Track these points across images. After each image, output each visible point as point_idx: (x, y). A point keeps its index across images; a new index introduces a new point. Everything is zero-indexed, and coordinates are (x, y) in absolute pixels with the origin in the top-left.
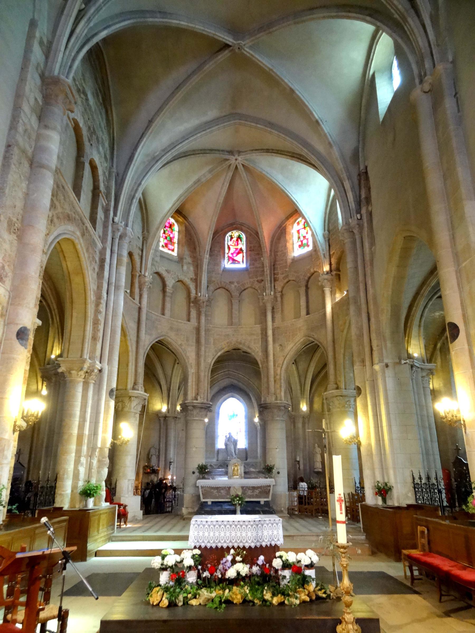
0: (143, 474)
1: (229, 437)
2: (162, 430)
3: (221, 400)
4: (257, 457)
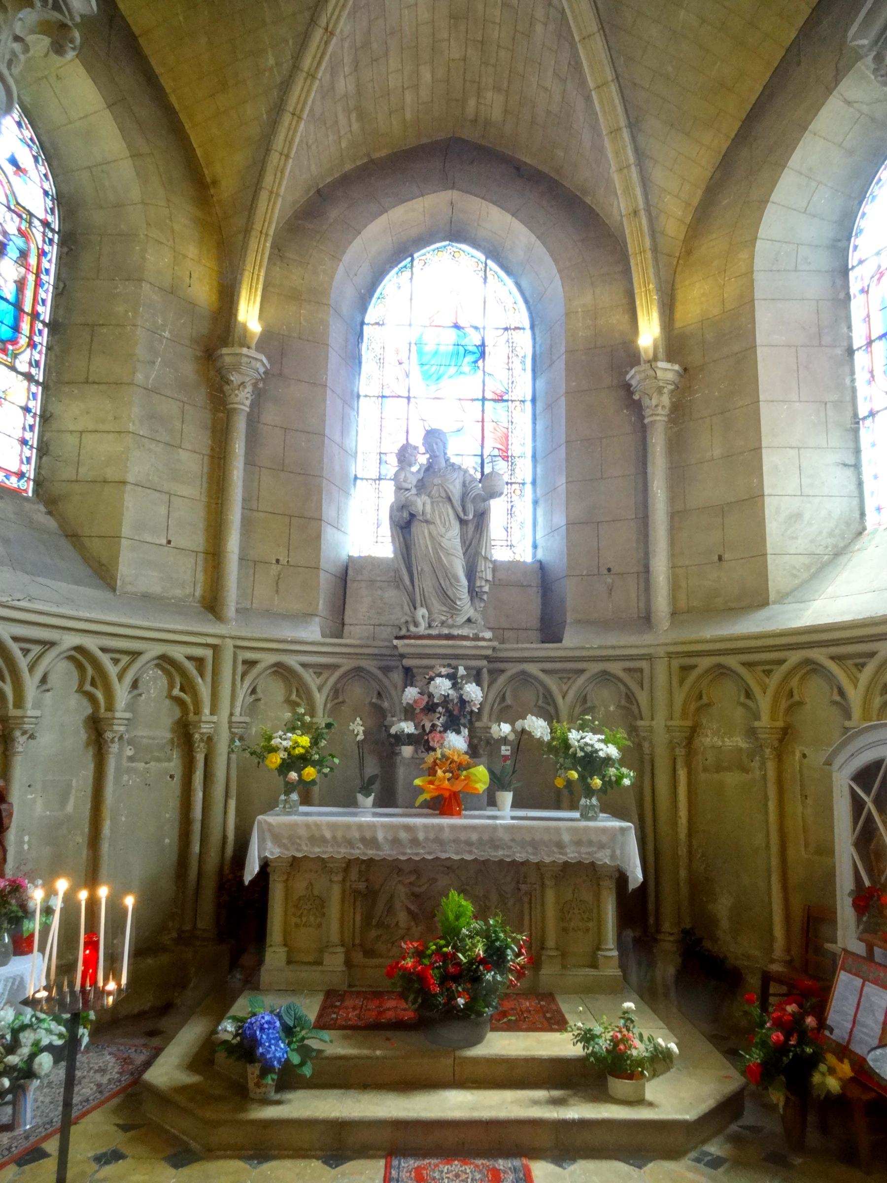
1: (429, 468)
3: (376, 232)
4: (646, 620)
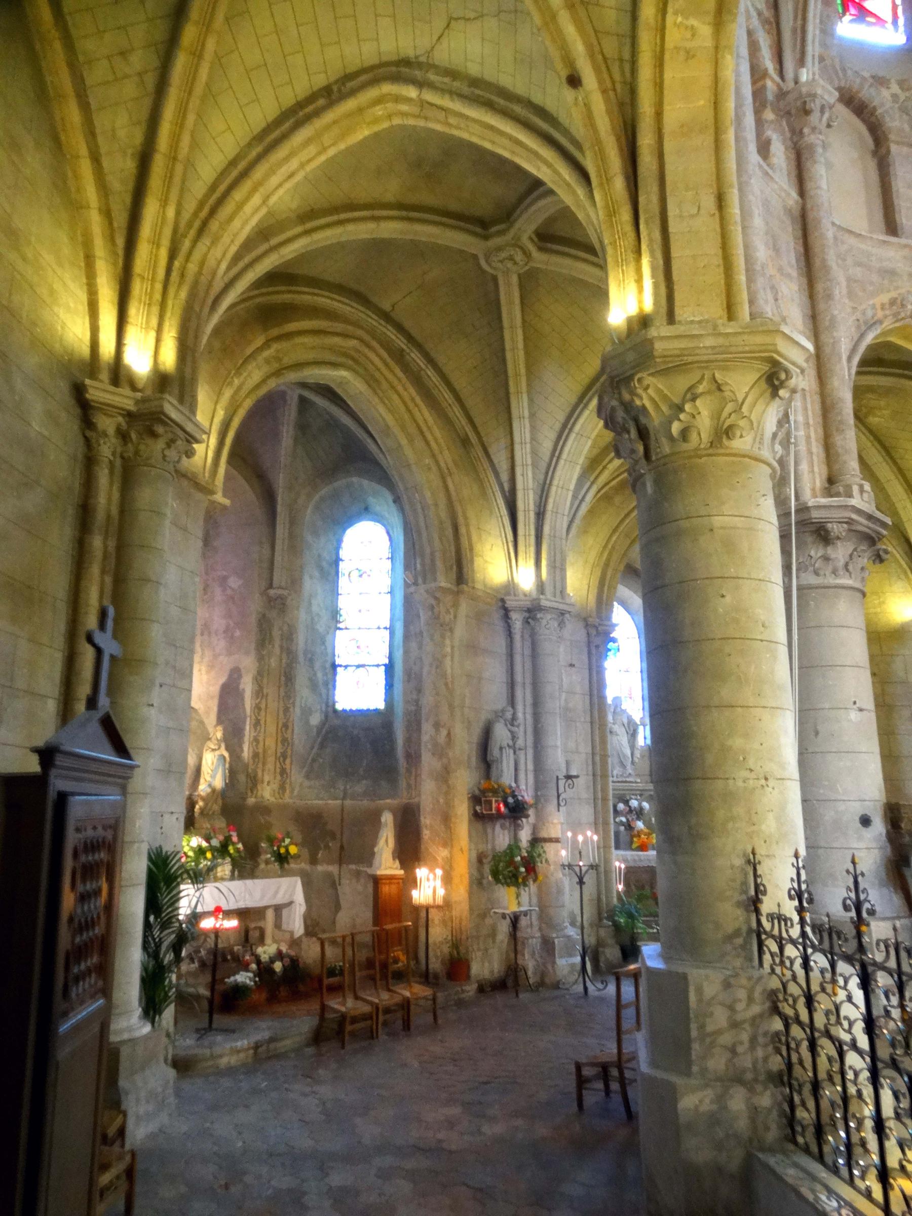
0: (470, 821)
2: (518, 659)
